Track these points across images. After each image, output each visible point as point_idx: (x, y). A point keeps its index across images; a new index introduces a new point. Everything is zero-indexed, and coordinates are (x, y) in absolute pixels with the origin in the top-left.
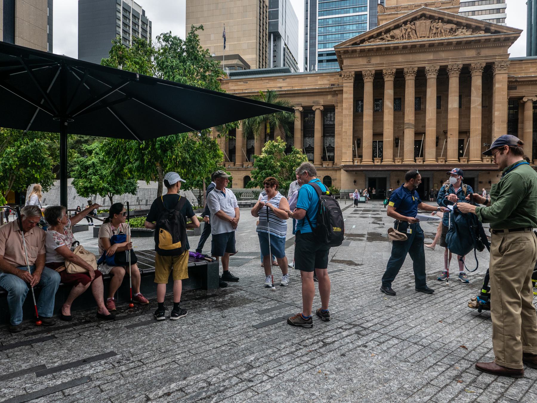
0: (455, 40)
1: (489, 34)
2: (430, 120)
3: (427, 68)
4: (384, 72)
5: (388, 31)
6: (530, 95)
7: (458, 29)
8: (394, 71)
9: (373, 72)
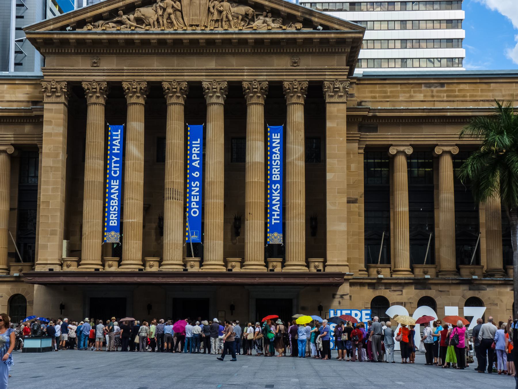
0: (250, 36)
1: (311, 30)
2: (212, 183)
3: (205, 85)
4: (125, 85)
5: (130, 9)
6: (401, 143)
7: (257, 16)
8: (144, 85)
9: (104, 85)
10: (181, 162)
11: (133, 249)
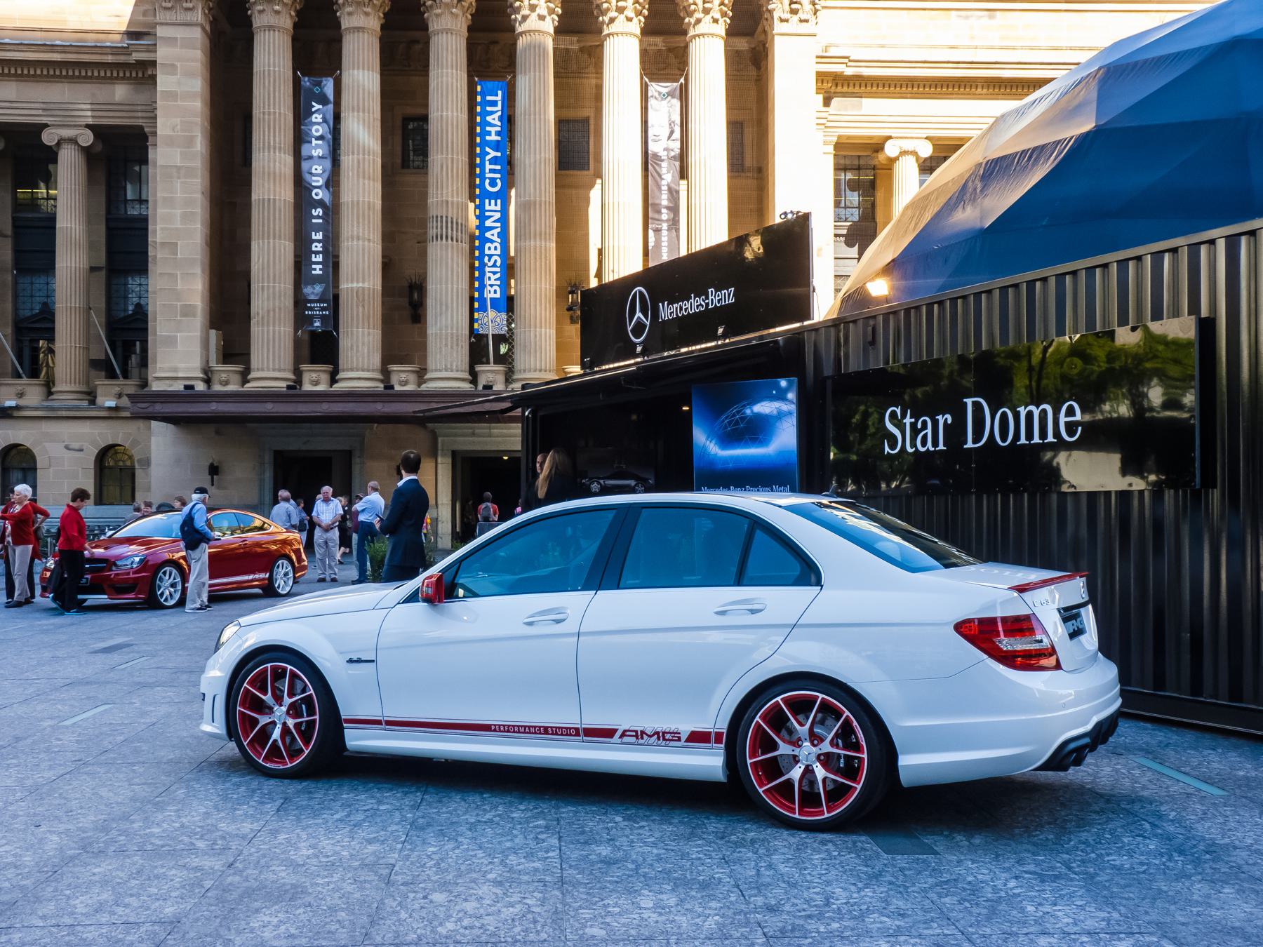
10: (463, 158)
11: (361, 346)
